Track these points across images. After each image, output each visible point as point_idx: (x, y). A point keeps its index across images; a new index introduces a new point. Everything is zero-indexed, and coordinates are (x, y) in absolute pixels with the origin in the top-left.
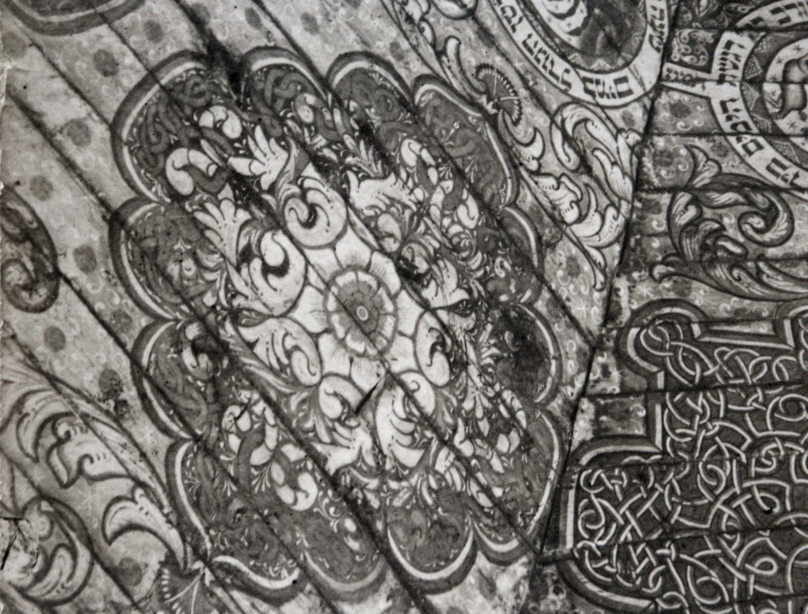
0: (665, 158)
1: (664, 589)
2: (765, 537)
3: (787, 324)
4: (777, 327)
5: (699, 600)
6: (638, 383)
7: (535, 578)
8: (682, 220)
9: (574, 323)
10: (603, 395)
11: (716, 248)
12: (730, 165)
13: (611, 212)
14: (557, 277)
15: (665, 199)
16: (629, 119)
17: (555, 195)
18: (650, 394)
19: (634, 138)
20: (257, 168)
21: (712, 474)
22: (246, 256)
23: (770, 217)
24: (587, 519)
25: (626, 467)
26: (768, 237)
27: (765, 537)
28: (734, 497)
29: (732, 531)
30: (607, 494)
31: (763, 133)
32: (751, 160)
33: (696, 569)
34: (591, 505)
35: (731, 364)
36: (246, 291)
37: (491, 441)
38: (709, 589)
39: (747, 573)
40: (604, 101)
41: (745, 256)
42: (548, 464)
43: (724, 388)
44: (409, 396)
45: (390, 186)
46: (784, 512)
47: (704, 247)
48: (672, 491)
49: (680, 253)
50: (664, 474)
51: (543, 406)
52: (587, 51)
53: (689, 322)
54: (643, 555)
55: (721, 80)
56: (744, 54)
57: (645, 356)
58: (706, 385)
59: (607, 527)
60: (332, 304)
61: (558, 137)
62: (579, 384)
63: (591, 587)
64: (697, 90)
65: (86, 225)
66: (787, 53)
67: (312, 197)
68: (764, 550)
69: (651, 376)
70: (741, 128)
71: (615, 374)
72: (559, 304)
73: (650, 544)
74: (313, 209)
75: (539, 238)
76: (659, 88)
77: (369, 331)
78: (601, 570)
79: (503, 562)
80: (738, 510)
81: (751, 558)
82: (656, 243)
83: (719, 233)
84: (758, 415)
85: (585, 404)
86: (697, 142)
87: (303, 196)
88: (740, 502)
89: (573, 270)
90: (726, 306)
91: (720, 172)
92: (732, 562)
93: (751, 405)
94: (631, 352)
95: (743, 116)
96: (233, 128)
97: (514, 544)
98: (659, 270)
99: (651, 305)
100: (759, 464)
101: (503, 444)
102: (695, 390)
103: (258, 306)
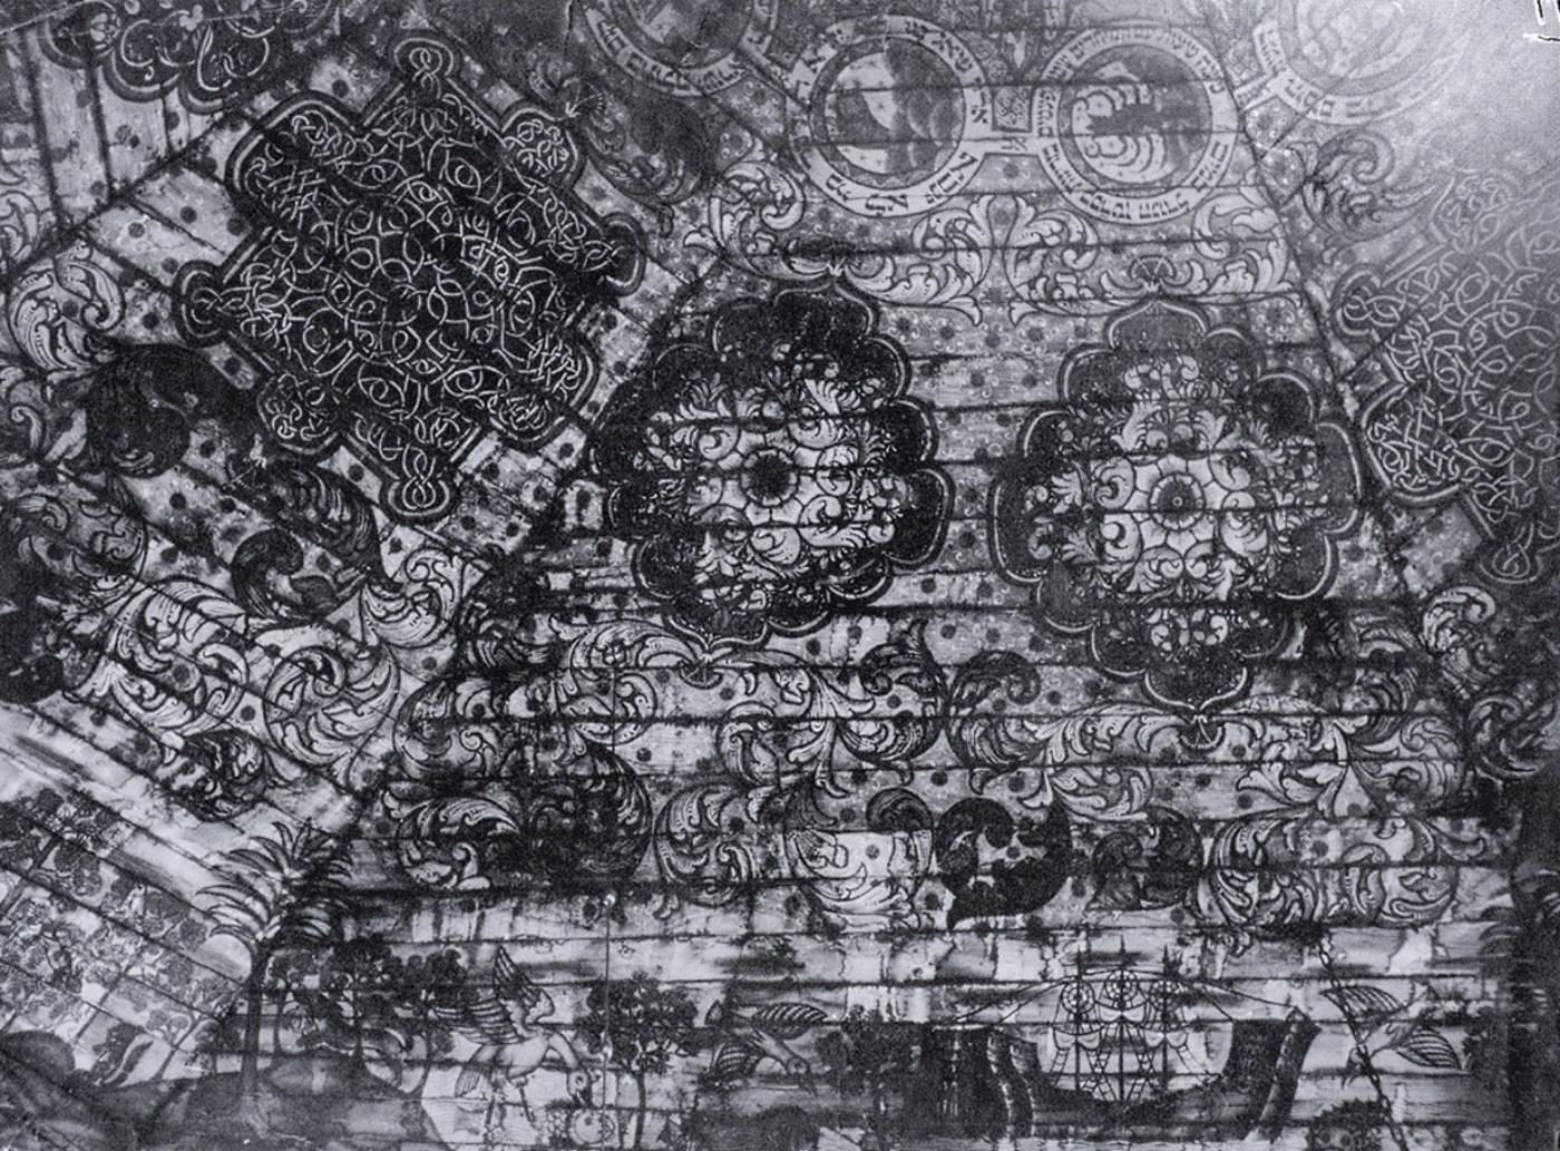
2: (1509, 391)
3: (1433, 227)
4: (1428, 236)
5: (1489, 461)
8: (1318, 208)
12: (1322, 136)
15: (1298, 198)
16: (1240, 170)
17: (1230, 287)
21: (1448, 375)
23: (1372, 156)
26: (1379, 173)
28: (1471, 380)
31: (1327, 92)
32: (1334, 120)
33: (1477, 445)
35: (1413, 289)
37: (1300, 477)
38: (1492, 451)
40: (1212, 183)
41: (1373, 201)
42: (1344, 447)
43: (1418, 311)
44: (1237, 511)
46: (1511, 365)
47: (1345, 216)
55: (1275, 74)
56: (1276, 36)
58: (1407, 317)
60: (1158, 517)
61: (1204, 247)
63: (1418, 499)
64: (1265, 95)
68: (1511, 401)
70: (1311, 100)
76: (1242, 118)
77: (1188, 508)
79: (1355, 531)
81: (1507, 410)
82: (1313, 239)
86: (1289, 138)
88: (1477, 380)
91: (1320, 149)
93: (1443, 309)
94: (1346, 330)
95: (1307, 89)
98: (1327, 255)
99: (1338, 285)
101: (1308, 471)
102: (1400, 329)
103: (1125, 568)
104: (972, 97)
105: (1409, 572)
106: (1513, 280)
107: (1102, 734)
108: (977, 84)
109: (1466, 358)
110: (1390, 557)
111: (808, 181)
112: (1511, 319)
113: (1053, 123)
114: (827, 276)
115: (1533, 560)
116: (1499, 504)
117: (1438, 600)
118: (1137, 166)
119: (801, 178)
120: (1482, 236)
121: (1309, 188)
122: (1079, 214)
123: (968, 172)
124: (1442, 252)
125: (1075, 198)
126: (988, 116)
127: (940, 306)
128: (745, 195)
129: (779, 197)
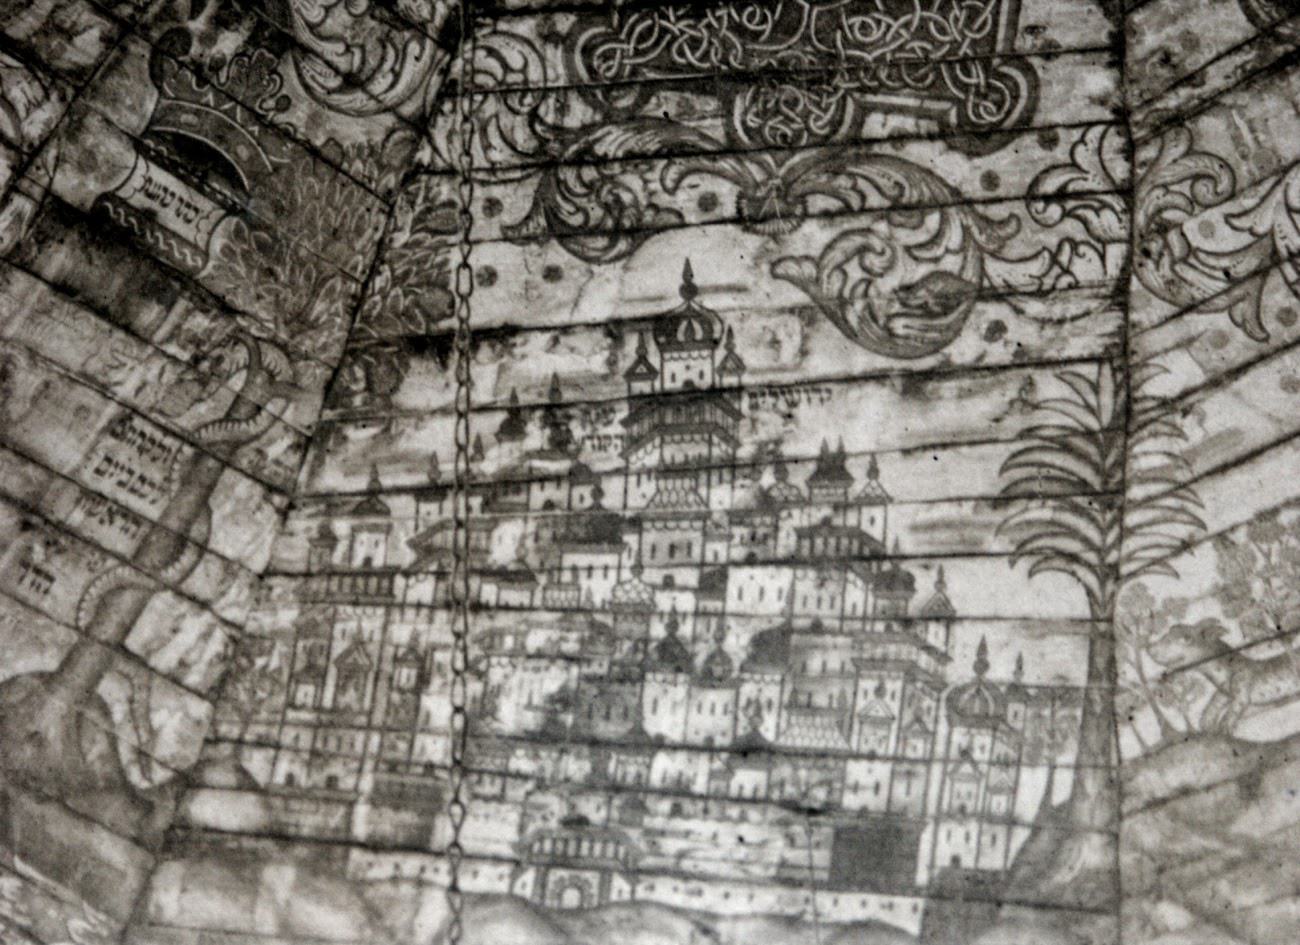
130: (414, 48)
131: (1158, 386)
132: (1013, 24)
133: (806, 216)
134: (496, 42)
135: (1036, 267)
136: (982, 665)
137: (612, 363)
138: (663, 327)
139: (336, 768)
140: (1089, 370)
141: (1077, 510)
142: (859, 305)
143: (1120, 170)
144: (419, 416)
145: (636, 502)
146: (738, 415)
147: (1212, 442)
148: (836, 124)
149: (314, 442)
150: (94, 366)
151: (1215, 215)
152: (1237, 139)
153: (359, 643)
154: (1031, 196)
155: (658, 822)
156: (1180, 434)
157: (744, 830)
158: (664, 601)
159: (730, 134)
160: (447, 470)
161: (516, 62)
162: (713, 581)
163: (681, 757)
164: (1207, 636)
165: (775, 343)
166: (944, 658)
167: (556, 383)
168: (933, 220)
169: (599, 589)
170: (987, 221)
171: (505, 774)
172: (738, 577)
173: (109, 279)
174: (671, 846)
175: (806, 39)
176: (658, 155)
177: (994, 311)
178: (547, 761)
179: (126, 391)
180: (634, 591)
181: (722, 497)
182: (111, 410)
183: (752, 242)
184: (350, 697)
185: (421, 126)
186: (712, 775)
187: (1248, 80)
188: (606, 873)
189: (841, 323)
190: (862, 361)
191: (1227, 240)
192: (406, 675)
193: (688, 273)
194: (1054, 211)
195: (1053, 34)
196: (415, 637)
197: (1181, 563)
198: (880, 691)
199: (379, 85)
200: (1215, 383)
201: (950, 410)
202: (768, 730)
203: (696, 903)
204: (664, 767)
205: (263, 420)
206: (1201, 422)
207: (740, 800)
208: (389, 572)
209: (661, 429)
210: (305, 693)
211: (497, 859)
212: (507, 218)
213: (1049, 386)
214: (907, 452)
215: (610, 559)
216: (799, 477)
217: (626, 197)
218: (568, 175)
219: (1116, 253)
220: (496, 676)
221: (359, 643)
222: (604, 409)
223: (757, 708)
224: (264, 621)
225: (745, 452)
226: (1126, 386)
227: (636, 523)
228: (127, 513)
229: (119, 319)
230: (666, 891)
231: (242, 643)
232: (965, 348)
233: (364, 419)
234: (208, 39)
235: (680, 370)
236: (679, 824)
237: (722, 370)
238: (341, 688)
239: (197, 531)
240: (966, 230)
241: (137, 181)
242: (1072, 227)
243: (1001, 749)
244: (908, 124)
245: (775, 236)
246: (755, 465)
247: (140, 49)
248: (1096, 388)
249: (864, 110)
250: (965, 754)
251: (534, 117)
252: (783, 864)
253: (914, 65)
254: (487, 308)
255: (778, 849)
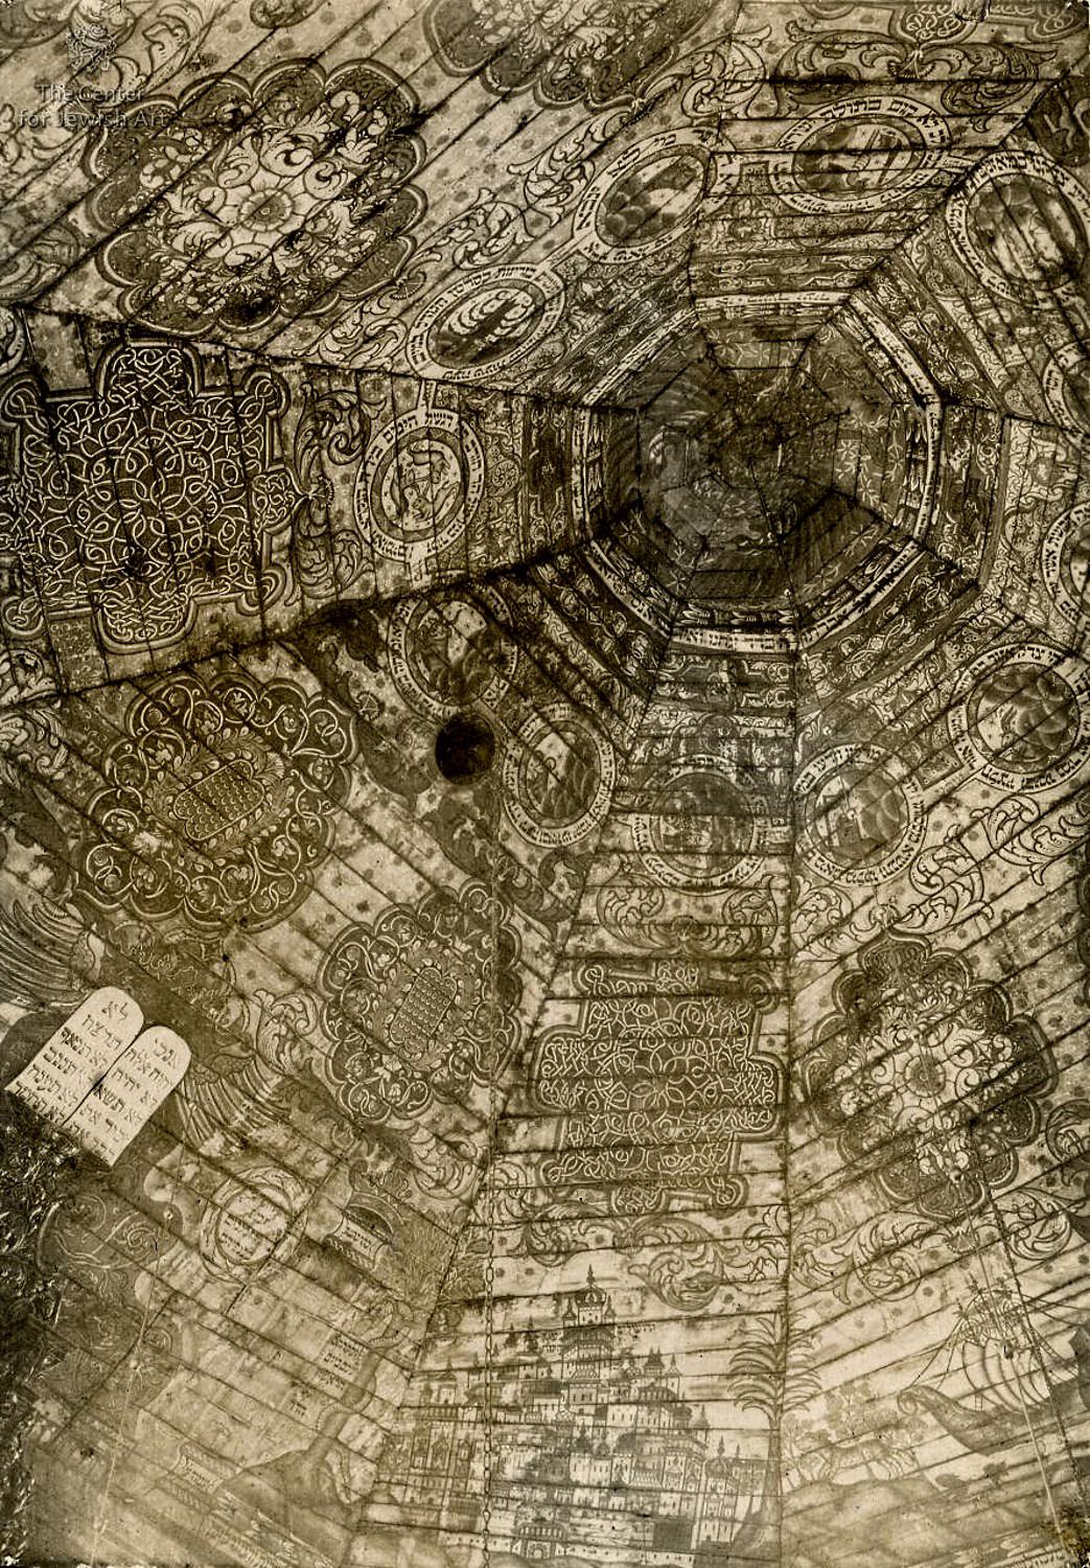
0: (377, 386)
1: (110, 404)
2: (149, 464)
4: (279, 460)
5: (107, 426)
6: (237, 379)
7: (107, 326)
8: (339, 399)
9: (271, 339)
10: (227, 360)
11: (324, 421)
12: (376, 424)
13: (342, 357)
14: (298, 327)
15: (353, 388)
16: (400, 362)
17: (349, 322)
18: (231, 387)
19: (388, 367)
20: (350, 145)
21: (184, 428)
22: (296, 140)
23: (347, 451)
24: (150, 355)
25: (184, 375)
26: (334, 450)
27: (149, 464)
28: (172, 443)
29: (151, 443)
30: (166, 366)
31: (397, 442)
33: (124, 425)
34: (158, 356)
36: (274, 141)
37: (193, 293)
38: (113, 432)
39: (126, 454)
40: (409, 347)
42: (182, 329)
43: (238, 432)
44: (217, 242)
45: (346, 225)
46: (165, 474)
47: (324, 413)
48: (171, 405)
49: (319, 399)
50: (182, 400)
51: (217, 323)
52: (439, 336)
53: (278, 408)
54: (131, 390)
55: (428, 415)
56: (445, 427)
57: (254, 383)
58: (239, 421)
59: (146, 367)
60: (269, 193)
62: (232, 344)
64: (422, 402)
65: (307, 44)
66: (448, 452)
67: (336, 178)
68: (141, 463)
69: (242, 387)
71: (241, 366)
72: (282, 329)
73: (138, 394)
74: (328, 179)
75: (322, 315)
76: (420, 379)
77: (254, 215)
78: (119, 365)
79: (119, 304)
80: (164, 446)
81: (135, 455)
82: (324, 385)
83: (334, 421)
84: (223, 453)
85: (221, 349)
86: (389, 404)
87: (335, 173)
89: (303, 337)
90: (289, 429)
92: (131, 445)
94: (256, 374)
95: (407, 430)
96: (374, 130)
97: (131, 311)
98: (308, 388)
99: (285, 384)
100: (193, 456)
101: (192, 300)
102: (234, 413)
103: (265, 148)
104: (603, 249)
105: (55, 322)
106: (219, 501)
107: (165, 38)
108: (604, 257)
109: (188, 447)
110: (79, 316)
111: (690, 126)
112: (194, 488)
113: (540, 284)
114: (642, 95)
115: (14, 420)
116: (71, 417)
117: (19, 332)
118: (466, 313)
119: (696, 122)
120: (258, 495)
121: (354, 399)
122: (486, 266)
123: (578, 220)
124: (263, 461)
125: (494, 270)
126: (586, 253)
127: (544, 152)
128: (734, 81)
129: (706, 100)
130: (467, 1169)
131: (801, 1324)
132: (737, 1159)
133: (644, 1246)
134: (505, 1166)
135: (747, 1270)
136: (721, 1450)
137: (556, 1312)
138: (579, 1295)
139: (432, 1495)
140: (770, 1317)
141: (764, 1380)
142: (668, 1286)
143: (785, 1226)
144: (469, 1336)
145: (567, 1375)
146: (613, 1337)
147: (823, 1350)
148: (657, 1204)
149: (422, 1347)
150: (324, 1313)
151: (827, 1247)
152: (837, 1214)
153: (442, 1438)
154: (745, 1238)
155: (576, 1520)
156: (809, 1346)
157: (614, 1524)
158: (579, 1420)
159: (610, 1208)
160: (482, 1360)
161: (514, 1175)
162: (601, 1411)
163: (587, 1490)
164: (821, 1436)
165: (630, 1303)
166: (705, 1447)
167: (531, 1322)
168: (701, 1248)
169: (550, 1415)
170: (725, 1249)
171: (508, 1498)
172: (612, 1410)
173: (331, 1273)
174: (582, 1531)
175: (644, 1166)
176: (577, 1218)
177: (728, 1290)
178: (527, 1491)
179: (337, 1324)
180: (565, 1417)
181: (606, 1373)
182: (332, 1332)
183: (619, 1258)
184: (438, 1463)
185: (471, 1204)
186: (601, 1499)
187: (843, 1185)
188: (553, 1543)
189: (660, 1295)
190: (669, 1312)
191: (833, 1259)
192: (464, 1453)
193: (591, 1272)
194: (755, 1244)
195: (754, 1164)
196: (468, 1436)
197: (811, 1404)
198: (676, 1462)
199: (451, 1187)
200: (827, 1323)
201: (708, 1334)
202: (626, 1479)
203: (593, 1557)
204: (579, 1495)
205: (399, 1337)
206: (820, 1339)
207: (613, 1511)
208: (456, 1406)
209: (578, 1342)
210: (419, 1460)
211: (505, 1536)
212: (509, 1247)
213: (752, 1324)
214: (688, 1353)
215: (556, 1401)
216: (640, 1364)
217: (563, 1237)
218: (537, 1227)
219: (782, 1264)
220: (504, 1454)
221: (442, 1438)
222: (553, 1333)
223: (621, 1469)
224: (399, 1428)
225: (615, 1354)
226: (787, 1326)
227: (567, 1385)
228: (338, 1379)
229: (333, 1291)
230: (580, 1551)
231: (390, 1438)
232: (715, 1306)
233: (444, 1337)
234: (375, 1165)
235: (586, 1316)
236: (586, 1521)
237: (606, 1315)
238: (434, 1459)
239: (370, 1388)
240: (716, 1253)
241: (343, 1229)
242: (763, 1252)
243: (729, 1488)
244: (690, 1204)
245: (630, 1255)
246: (620, 1359)
247: (344, 1169)
248: (773, 1325)
249: (670, 1198)
250: (714, 1490)
251: (521, 1200)
252: (632, 1539)
253: (692, 1178)
254: (500, 1287)
255: (630, 1533)
